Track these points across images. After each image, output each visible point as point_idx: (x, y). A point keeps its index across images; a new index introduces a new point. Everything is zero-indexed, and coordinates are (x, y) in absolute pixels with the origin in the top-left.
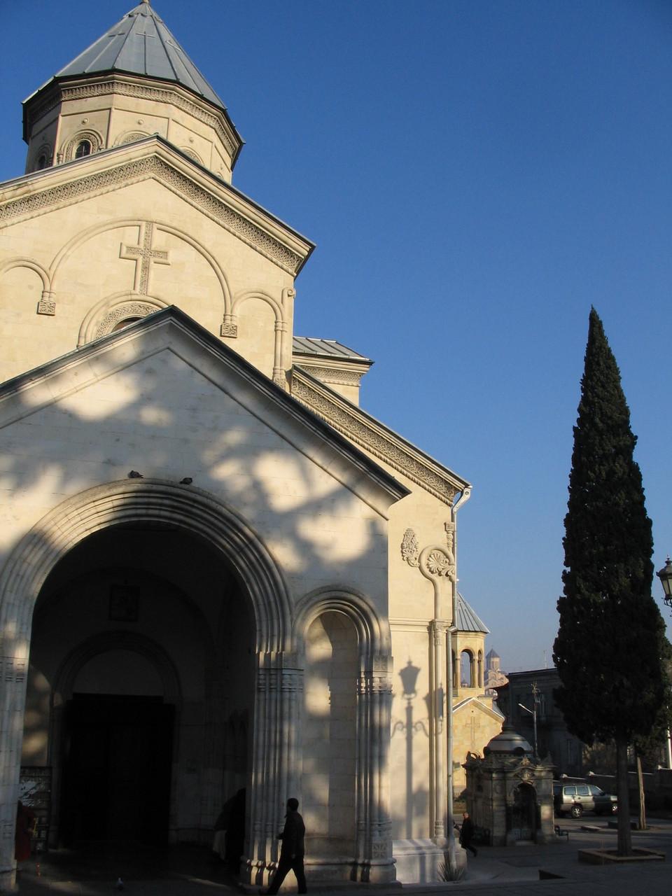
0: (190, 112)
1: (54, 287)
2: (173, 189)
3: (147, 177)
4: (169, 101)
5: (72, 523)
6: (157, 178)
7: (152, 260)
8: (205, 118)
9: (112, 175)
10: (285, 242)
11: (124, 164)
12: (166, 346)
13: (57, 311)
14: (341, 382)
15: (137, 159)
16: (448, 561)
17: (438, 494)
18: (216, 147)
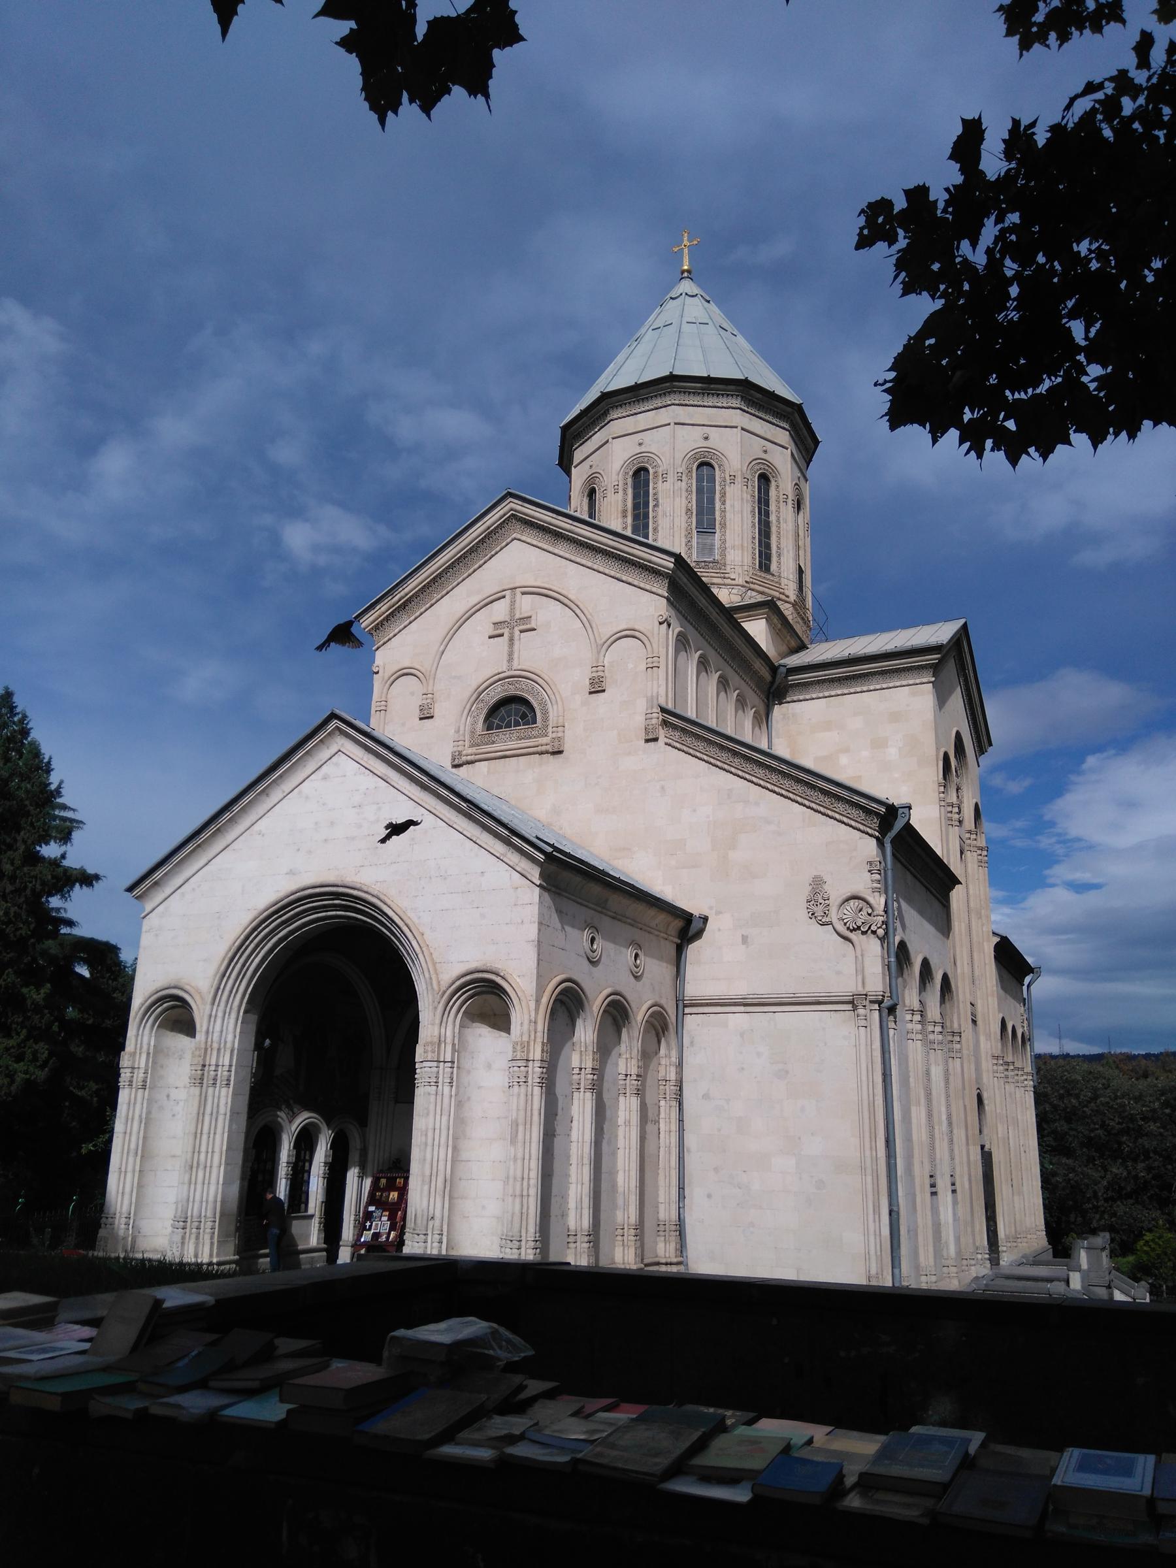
0: (702, 404)
1: (430, 688)
2: (535, 542)
3: (510, 539)
4: (669, 403)
5: (263, 934)
6: (519, 536)
7: (517, 630)
8: (723, 401)
9: (476, 550)
10: (650, 562)
11: (483, 535)
12: (336, 751)
13: (437, 711)
14: (904, 683)
15: (496, 525)
16: (870, 911)
17: (853, 823)
18: (743, 429)
